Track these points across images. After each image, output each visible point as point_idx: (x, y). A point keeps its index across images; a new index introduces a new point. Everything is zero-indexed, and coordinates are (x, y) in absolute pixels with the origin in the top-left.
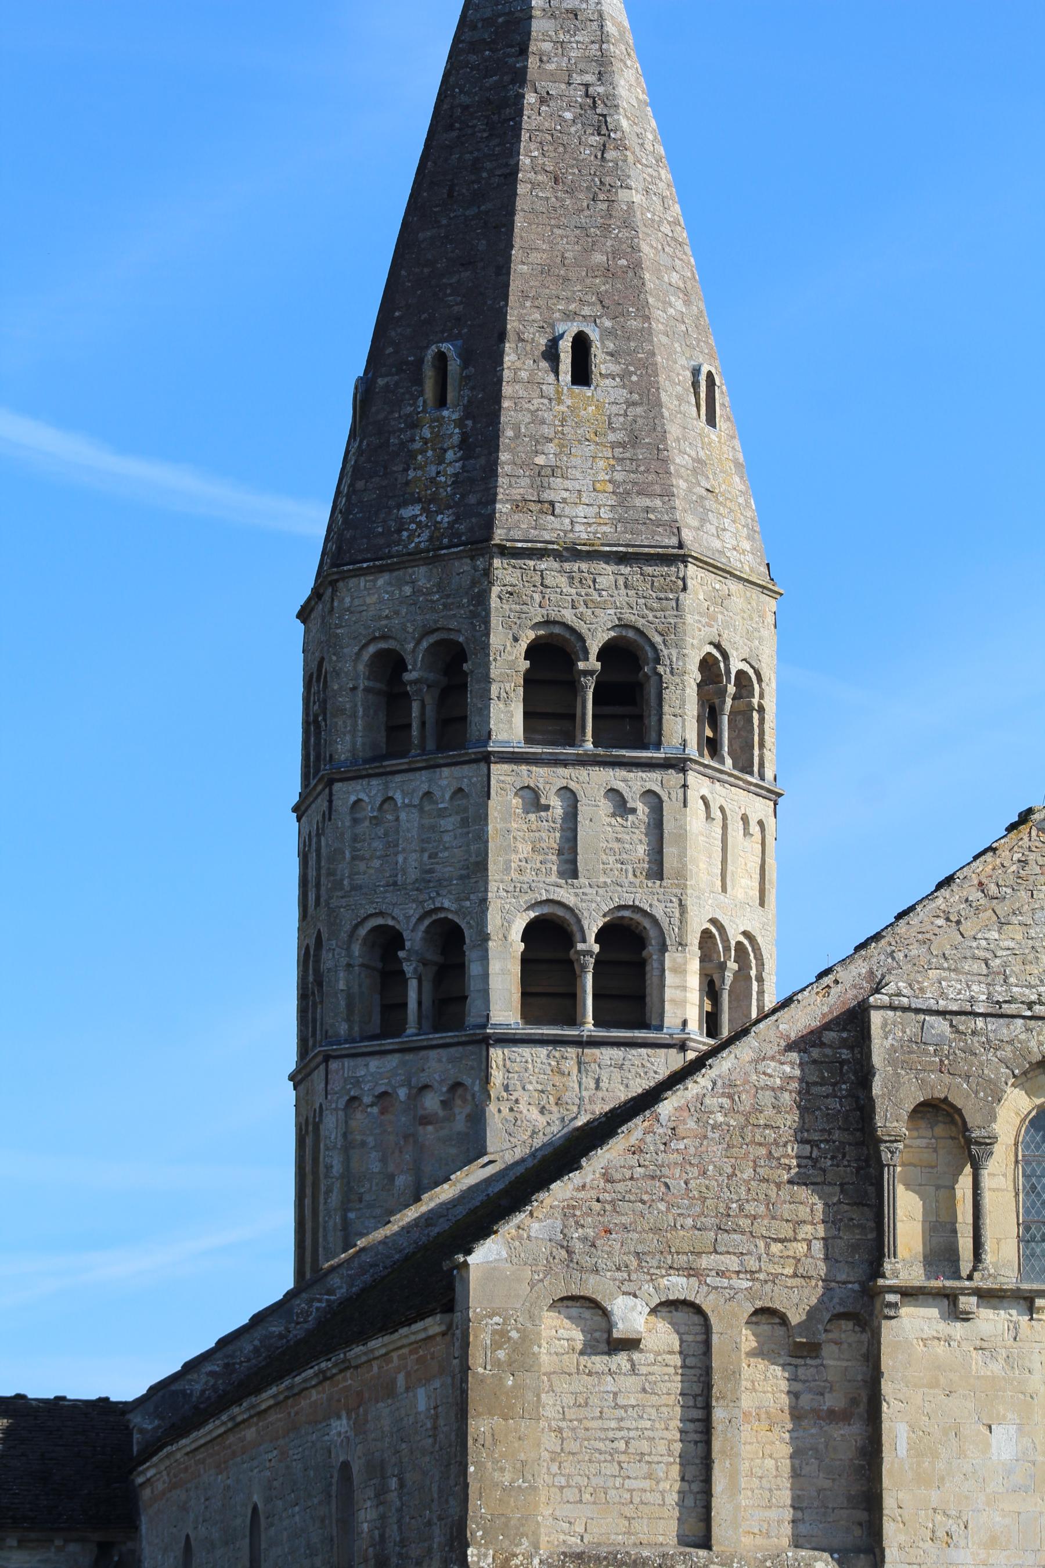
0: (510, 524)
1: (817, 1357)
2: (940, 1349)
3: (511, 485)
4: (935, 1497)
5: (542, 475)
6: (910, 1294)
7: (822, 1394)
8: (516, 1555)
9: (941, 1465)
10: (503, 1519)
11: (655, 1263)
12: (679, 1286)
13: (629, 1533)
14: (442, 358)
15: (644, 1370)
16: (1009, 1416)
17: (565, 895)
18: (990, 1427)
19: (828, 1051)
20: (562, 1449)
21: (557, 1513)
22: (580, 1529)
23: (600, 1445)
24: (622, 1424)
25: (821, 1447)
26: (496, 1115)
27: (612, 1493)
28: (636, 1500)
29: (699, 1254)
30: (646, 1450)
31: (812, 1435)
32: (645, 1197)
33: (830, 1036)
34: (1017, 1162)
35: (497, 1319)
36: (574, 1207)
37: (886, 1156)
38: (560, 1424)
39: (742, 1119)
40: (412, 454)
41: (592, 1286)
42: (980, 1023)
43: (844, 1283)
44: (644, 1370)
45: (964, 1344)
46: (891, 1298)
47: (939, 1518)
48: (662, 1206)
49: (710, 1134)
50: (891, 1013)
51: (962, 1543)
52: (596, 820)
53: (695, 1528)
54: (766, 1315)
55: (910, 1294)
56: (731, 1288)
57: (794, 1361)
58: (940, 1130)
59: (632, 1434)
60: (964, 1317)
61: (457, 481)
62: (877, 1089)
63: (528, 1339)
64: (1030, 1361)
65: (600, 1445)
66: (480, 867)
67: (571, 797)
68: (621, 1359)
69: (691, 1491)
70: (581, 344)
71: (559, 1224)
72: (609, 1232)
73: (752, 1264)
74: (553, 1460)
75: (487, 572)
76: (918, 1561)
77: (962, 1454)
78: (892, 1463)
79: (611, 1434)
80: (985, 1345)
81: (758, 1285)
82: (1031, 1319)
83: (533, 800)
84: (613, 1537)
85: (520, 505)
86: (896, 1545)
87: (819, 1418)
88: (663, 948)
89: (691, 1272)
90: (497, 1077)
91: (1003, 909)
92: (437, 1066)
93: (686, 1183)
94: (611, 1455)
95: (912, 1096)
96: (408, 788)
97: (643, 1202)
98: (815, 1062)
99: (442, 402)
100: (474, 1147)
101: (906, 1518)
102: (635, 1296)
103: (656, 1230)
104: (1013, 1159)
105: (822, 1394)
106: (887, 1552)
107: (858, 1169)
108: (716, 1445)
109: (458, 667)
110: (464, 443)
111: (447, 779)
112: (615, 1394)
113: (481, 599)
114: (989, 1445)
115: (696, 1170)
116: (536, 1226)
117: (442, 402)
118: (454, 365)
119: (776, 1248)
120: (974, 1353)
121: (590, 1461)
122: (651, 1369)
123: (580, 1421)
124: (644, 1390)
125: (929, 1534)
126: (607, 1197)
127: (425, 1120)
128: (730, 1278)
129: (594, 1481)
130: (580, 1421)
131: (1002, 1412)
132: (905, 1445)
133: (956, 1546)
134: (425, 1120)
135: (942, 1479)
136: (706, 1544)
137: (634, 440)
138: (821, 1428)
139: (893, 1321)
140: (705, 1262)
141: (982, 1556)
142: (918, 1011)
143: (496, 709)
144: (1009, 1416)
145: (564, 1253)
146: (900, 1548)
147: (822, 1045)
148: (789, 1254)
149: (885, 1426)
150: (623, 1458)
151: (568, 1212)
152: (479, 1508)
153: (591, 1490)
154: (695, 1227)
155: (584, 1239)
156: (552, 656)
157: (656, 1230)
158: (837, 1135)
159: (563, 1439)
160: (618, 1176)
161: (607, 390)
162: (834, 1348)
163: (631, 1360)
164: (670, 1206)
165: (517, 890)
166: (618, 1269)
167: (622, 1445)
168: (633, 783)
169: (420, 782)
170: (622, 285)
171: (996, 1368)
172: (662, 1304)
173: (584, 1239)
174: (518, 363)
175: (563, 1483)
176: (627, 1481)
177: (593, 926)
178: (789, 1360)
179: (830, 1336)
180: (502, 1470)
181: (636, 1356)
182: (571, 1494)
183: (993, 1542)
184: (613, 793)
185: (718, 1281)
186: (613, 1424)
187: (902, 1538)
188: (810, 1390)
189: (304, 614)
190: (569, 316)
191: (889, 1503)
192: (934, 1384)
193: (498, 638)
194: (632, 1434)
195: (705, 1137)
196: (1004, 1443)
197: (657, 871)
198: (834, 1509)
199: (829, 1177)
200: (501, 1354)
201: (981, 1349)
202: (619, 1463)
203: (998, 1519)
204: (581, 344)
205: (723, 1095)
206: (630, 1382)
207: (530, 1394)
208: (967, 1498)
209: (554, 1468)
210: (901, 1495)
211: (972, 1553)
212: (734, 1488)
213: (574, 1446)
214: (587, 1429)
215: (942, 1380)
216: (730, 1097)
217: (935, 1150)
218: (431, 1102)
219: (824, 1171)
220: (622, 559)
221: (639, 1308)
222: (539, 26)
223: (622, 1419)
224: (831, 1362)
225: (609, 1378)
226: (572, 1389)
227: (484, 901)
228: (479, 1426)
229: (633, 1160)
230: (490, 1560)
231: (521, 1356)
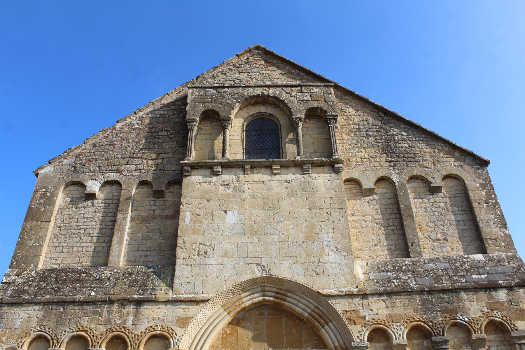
1: (164, 197)
2: (206, 186)
4: (200, 239)
6: (195, 167)
7: (164, 210)
8: (26, 271)
9: (204, 226)
10: (26, 257)
11: (105, 169)
12: (113, 176)
13: (79, 263)
15: (96, 205)
16: (234, 207)
18: (226, 212)
19: (178, 107)
20: (60, 234)
21: (52, 256)
22: (59, 262)
23: (75, 231)
24: (84, 224)
25: (162, 228)
27: (75, 248)
28: (84, 250)
29: (121, 165)
30: (92, 232)
31: (159, 224)
32: (106, 150)
33: (178, 103)
34: (243, 131)
35: (44, 190)
36: (80, 155)
37: (190, 127)
38: (61, 225)
39: (144, 127)
41: (80, 178)
42: (227, 89)
43: (175, 171)
44: (96, 205)
45: (216, 184)
46: (186, 168)
47: (201, 246)
48: (111, 153)
49: (132, 131)
50: (195, 90)
51: (211, 256)
55: (195, 167)
56: (132, 175)
57: (155, 199)
58: (214, 124)
59: (87, 227)
60: (216, 174)
62: (188, 108)
63: (54, 195)
64: (244, 188)
65: (75, 231)
68: (89, 203)
69: (106, 246)
71: (74, 160)
72: (90, 161)
73: (141, 167)
74: (55, 237)
76: (191, 264)
77: (213, 222)
78: (183, 227)
79: (79, 227)
80: (225, 183)
81: (142, 174)
82: (244, 174)
84: (72, 264)
86: (181, 258)
87: (162, 218)
89: (117, 171)
91: (240, 70)
93: (121, 145)
94: (78, 235)
95: (201, 109)
97: (105, 152)
98: (172, 109)
101: (187, 247)
102: (96, 180)
103: (107, 159)
104: (241, 130)
105: (164, 210)
106: (177, 261)
107: (183, 137)
108: (116, 227)
112: (84, 214)
114: (225, 218)
115: (125, 142)
116: (65, 161)
119: (150, 162)
120: (220, 187)
121: (70, 237)
122: (99, 205)
123: (69, 223)
124: (95, 212)
125: (197, 253)
126: (93, 151)
128: (132, 172)
129: (69, 244)
130: (69, 223)
131: (231, 206)
132: (189, 220)
133: (208, 257)
135: (204, 231)
136: (106, 265)
138: (163, 221)
139: (188, 178)
140: (123, 168)
141: (220, 261)
142: (205, 88)
144: (234, 207)
145: (73, 168)
146: (184, 259)
147: (175, 105)
149: (181, 213)
150: (82, 235)
153: (67, 247)
154: (122, 158)
155: (81, 164)
157: (107, 159)
158: (177, 128)
159: (61, 230)
160: (97, 145)
162: (171, 194)
163: (93, 203)
164: (114, 152)
166: (92, 172)
167: (83, 231)
171: (229, 191)
172: (105, 182)
173: (81, 164)
175: (57, 245)
176: (82, 244)
178: (153, 199)
179: (170, 190)
180: (31, 240)
181: (95, 201)
182: (58, 249)
183: (226, 255)
185: (127, 173)
186: (81, 224)
187: (184, 255)
188: (160, 209)
191: (180, 241)
192: (203, 197)
194: (87, 227)
195: (130, 132)
196: (232, 217)
198: (164, 251)
199: (173, 140)
200: (42, 201)
201: (224, 185)
202: (80, 237)
203: (228, 246)
205: (139, 120)
206: (91, 210)
207: (49, 213)
208: (214, 238)
209: (55, 240)
210: (185, 238)
211: (216, 260)
212: (121, 242)
213: (64, 232)
214: (71, 226)
215: (206, 196)
216: (141, 121)
217: (212, 129)
219: (171, 138)
221: (96, 184)
223: (85, 222)
224: (169, 199)
225: (83, 209)
226: (68, 213)
229: (104, 140)
230: (15, 272)
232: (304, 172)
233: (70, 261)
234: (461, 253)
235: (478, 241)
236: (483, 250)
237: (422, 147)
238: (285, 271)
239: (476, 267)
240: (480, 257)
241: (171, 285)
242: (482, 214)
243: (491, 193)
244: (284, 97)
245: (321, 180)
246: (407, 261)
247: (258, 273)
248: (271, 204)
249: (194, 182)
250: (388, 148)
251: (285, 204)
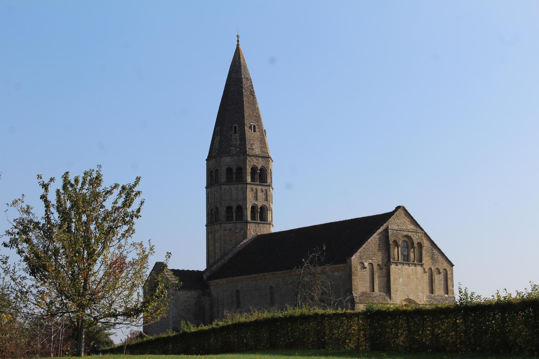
0: (249, 152)
3: (248, 146)
5: (252, 145)
12: (370, 261)
14: (235, 127)
17: (256, 203)
26: (248, 232)
40: (231, 140)
41: (363, 261)
52: (260, 194)
53: (372, 289)
54: (378, 265)
55: (393, 263)
61: (240, 145)
63: (357, 267)
66: (246, 198)
67: (257, 189)
70: (254, 126)
75: (246, 158)
83: (262, 191)
85: (249, 149)
88: (267, 211)
89: (372, 260)
90: (248, 227)
92: (239, 225)
95: (393, 240)
96: (233, 187)
99: (235, 132)
100: (245, 237)
109: (241, 171)
110: (240, 139)
111: (240, 186)
113: (246, 162)
117: (235, 132)
118: (237, 128)
127: (236, 233)
134: (236, 233)
137: (262, 141)
143: (248, 177)
148: (378, 259)
151: (360, 252)
152: (353, 287)
156: (254, 169)
161: (258, 133)
165: (250, 202)
168: (264, 188)
169: (236, 186)
170: (258, 118)
174: (247, 128)
177: (259, 207)
184: (252, 189)
189: (207, 160)
190: (252, 122)
193: (248, 167)
196: (401, 280)
197: (266, 200)
204: (254, 126)
218: (237, 230)
220: (262, 157)
222: (244, 80)
227: (246, 204)
228: (353, 277)
231: (356, 270)
232: (415, 266)
233: (364, 290)
234: (443, 293)
235: (447, 291)
236: (447, 294)
237: (440, 258)
238: (412, 297)
239: (446, 299)
240: (446, 295)
241: (390, 298)
242: (449, 281)
243: (452, 276)
244: (412, 237)
245: (419, 268)
246: (433, 295)
247: (407, 297)
248: (408, 277)
249: (393, 267)
250: (432, 258)
251: (412, 277)
